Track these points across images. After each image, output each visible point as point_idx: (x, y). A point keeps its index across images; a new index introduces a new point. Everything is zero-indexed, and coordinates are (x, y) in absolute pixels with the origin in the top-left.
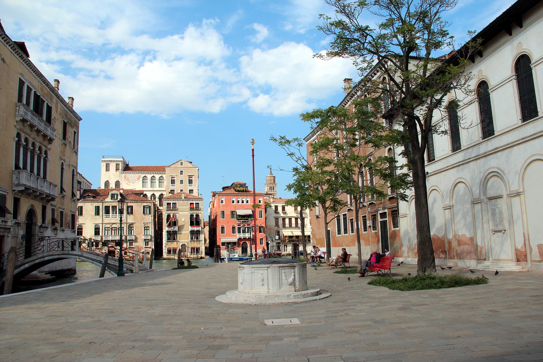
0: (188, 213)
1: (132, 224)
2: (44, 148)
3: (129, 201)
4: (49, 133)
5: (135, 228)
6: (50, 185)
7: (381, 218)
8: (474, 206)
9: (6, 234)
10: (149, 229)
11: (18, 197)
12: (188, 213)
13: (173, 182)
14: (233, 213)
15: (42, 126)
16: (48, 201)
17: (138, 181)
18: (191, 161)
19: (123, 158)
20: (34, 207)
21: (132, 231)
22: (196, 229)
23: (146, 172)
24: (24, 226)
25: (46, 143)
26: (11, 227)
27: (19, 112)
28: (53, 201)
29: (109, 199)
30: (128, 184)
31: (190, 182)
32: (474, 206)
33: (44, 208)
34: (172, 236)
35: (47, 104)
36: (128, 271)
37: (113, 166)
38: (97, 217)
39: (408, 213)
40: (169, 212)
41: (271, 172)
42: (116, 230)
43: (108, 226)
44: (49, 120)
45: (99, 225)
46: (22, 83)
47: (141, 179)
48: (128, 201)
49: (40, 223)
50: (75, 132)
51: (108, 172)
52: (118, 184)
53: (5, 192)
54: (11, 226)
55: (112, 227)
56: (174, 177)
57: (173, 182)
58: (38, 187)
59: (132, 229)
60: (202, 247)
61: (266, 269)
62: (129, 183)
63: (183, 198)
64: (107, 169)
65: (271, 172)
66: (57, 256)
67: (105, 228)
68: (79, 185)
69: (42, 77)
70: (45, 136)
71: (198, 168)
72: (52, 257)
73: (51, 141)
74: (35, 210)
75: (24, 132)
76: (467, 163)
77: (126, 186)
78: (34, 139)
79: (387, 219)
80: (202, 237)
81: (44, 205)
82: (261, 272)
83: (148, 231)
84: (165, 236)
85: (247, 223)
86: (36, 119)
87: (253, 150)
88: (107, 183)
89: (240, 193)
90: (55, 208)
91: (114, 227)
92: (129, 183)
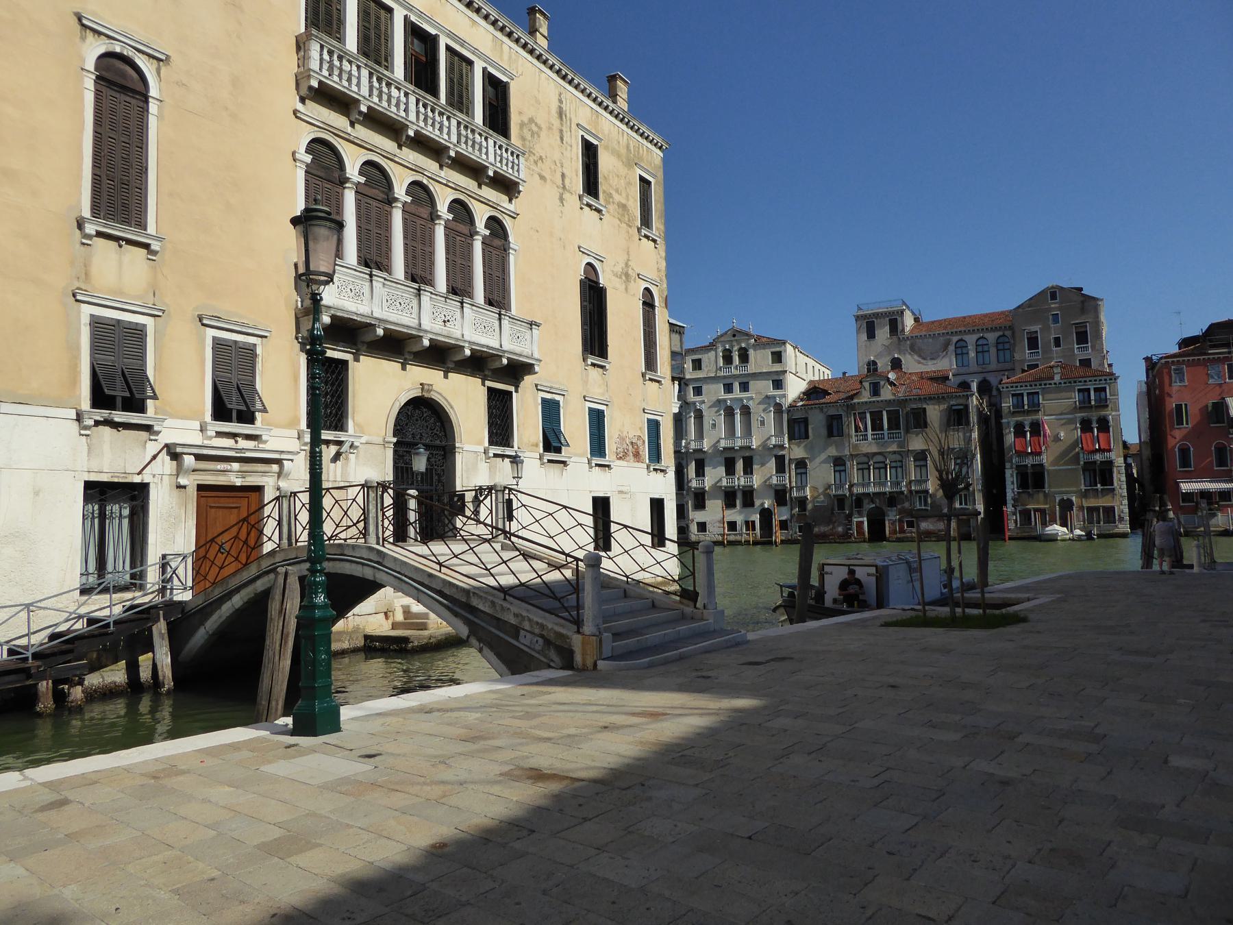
17: (945, 352)
30: (919, 363)
35: (484, 69)
36: (553, 654)
44: (498, 118)
47: (952, 348)
49: (480, 443)
62: (922, 361)
68: (676, 337)
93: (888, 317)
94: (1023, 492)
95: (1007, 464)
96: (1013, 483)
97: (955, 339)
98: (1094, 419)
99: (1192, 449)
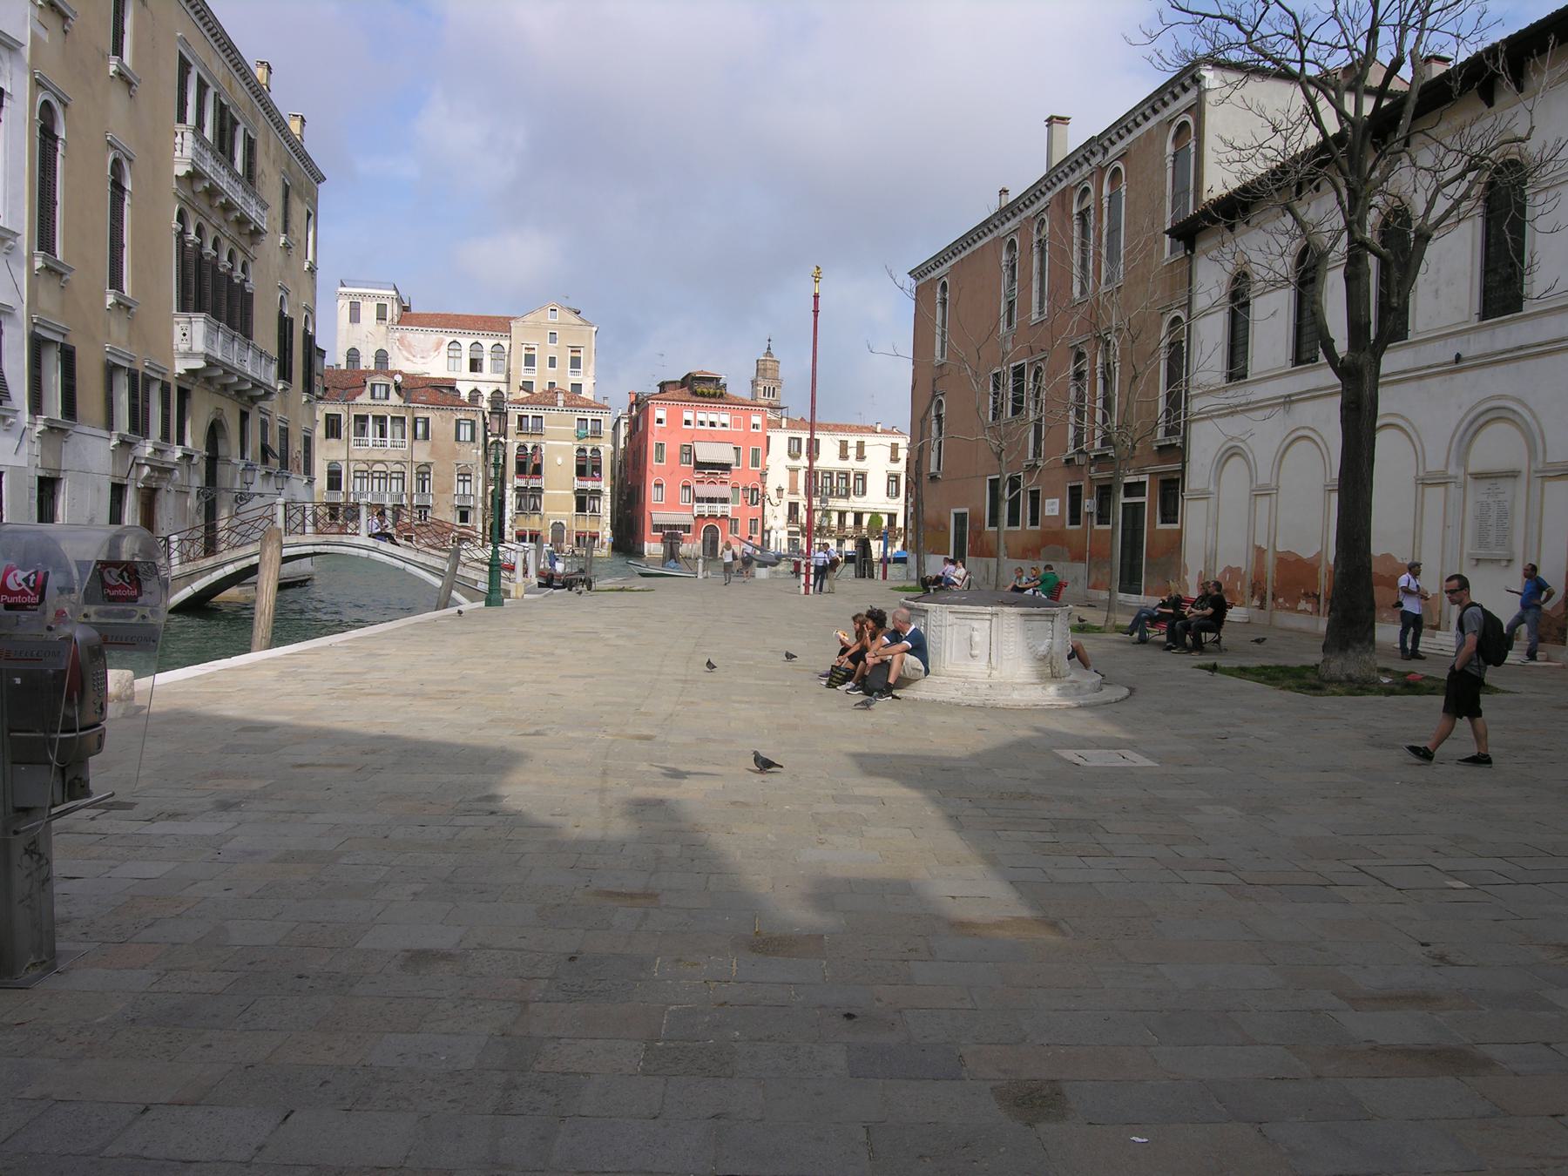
0: (571, 443)
1: (427, 465)
2: (240, 257)
3: (420, 405)
4: (253, 215)
5: (434, 475)
6: (261, 357)
7: (1126, 495)
8: (1423, 490)
9: (164, 484)
10: (470, 481)
11: (187, 386)
12: (572, 446)
13: (530, 360)
14: (688, 451)
15: (237, 196)
16: (254, 400)
17: (437, 353)
18: (578, 308)
19: (395, 289)
20: (222, 414)
21: (427, 482)
22: (590, 485)
23: (458, 331)
24: (203, 466)
25: (244, 242)
26: (176, 467)
27: (182, 151)
28: (267, 400)
29: (364, 398)
30: (408, 360)
31: (576, 363)
32: (1423, 490)
33: (244, 416)
34: (530, 499)
37: (368, 311)
38: (333, 441)
39: (1211, 488)
40: (523, 439)
41: (769, 348)
42: (386, 478)
43: (364, 467)
45: (340, 463)
46: (184, 66)
47: (444, 348)
48: (416, 405)
50: (309, 215)
51: (355, 325)
52: (382, 357)
53: (158, 372)
54: (176, 464)
55: (373, 469)
56: (534, 349)
57: (530, 360)
58: (235, 362)
59: (427, 476)
60: (605, 533)
61: (988, 617)
62: (411, 358)
63: (561, 403)
64: (355, 317)
65: (769, 348)
66: (311, 547)
67: (355, 471)
69: (232, 52)
70: (243, 221)
71: (595, 329)
72: (297, 548)
73: (257, 233)
74: (223, 421)
75: (195, 210)
76: (1420, 378)
77: (402, 363)
78: (218, 229)
79: (1145, 499)
80: (604, 507)
81: (245, 409)
82: (976, 624)
83: (467, 484)
84: (511, 499)
85: (721, 478)
86: (222, 172)
87: (816, 296)
88: (353, 355)
89: (706, 399)
90: (267, 418)
91: (380, 472)
92: (411, 358)
93: (376, 300)
94: (521, 513)
95: (508, 484)
96: (512, 503)
97: (451, 339)
98: (589, 449)
99: (664, 485)
